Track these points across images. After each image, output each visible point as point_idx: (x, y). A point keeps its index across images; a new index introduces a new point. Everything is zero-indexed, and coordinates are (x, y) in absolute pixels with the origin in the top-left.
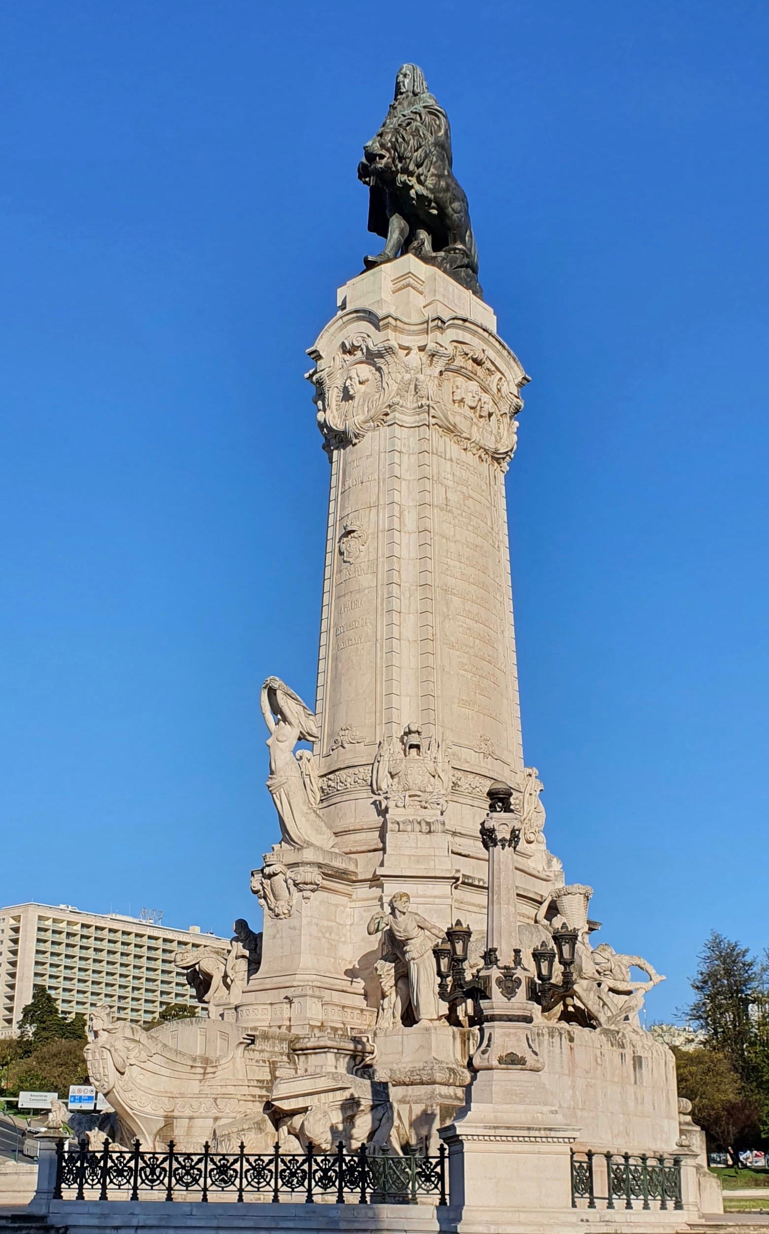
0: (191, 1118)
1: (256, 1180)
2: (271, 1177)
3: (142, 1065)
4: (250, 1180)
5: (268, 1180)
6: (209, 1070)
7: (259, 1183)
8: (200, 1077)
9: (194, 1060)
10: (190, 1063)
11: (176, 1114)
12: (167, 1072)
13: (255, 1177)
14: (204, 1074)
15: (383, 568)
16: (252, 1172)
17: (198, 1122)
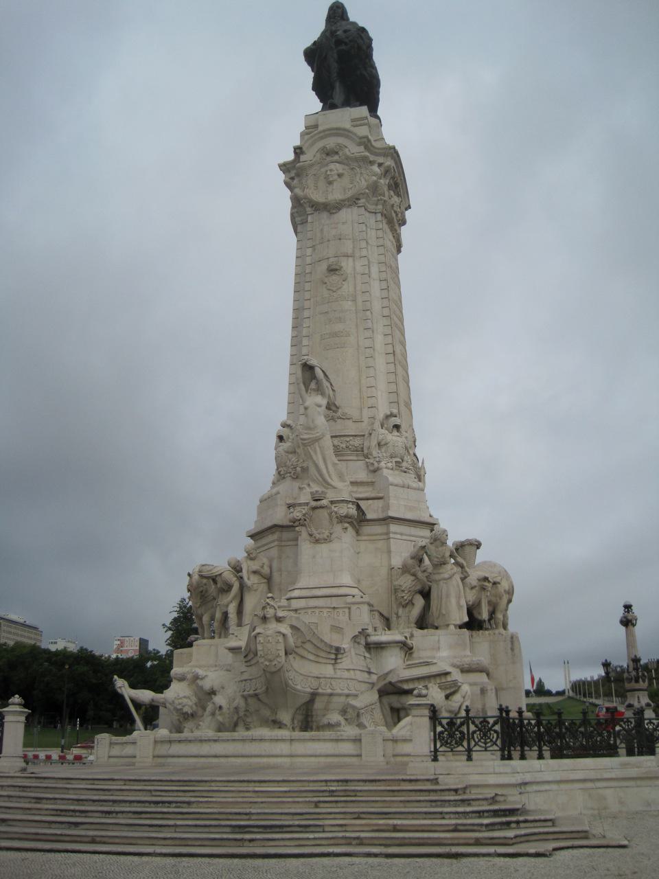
0: (331, 695)
1: (482, 741)
2: (498, 737)
3: (296, 650)
4: (477, 740)
5: (494, 740)
6: (340, 656)
7: (485, 743)
8: (333, 662)
9: (331, 646)
10: (328, 650)
11: (320, 691)
12: (312, 657)
13: (482, 738)
14: (336, 659)
15: (360, 300)
16: (478, 733)
17: (335, 699)
